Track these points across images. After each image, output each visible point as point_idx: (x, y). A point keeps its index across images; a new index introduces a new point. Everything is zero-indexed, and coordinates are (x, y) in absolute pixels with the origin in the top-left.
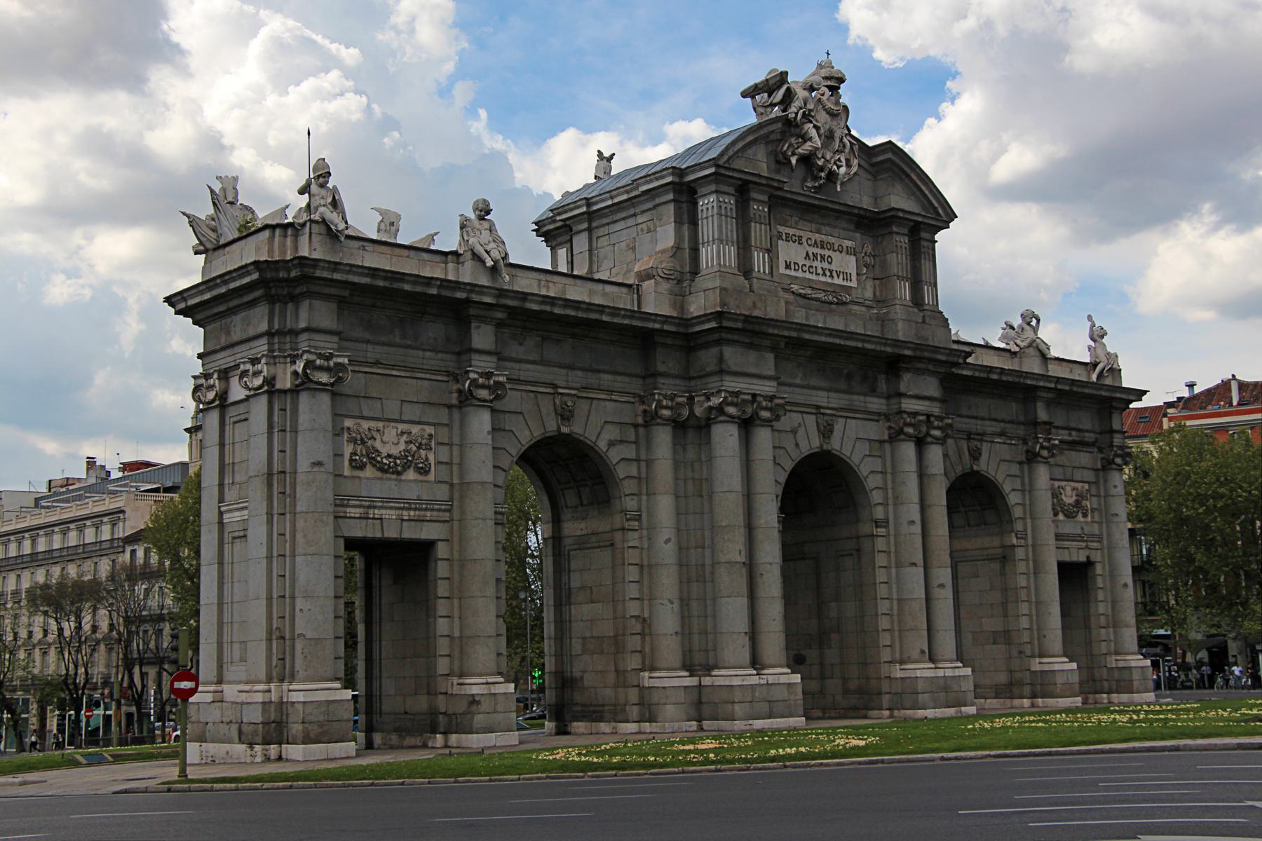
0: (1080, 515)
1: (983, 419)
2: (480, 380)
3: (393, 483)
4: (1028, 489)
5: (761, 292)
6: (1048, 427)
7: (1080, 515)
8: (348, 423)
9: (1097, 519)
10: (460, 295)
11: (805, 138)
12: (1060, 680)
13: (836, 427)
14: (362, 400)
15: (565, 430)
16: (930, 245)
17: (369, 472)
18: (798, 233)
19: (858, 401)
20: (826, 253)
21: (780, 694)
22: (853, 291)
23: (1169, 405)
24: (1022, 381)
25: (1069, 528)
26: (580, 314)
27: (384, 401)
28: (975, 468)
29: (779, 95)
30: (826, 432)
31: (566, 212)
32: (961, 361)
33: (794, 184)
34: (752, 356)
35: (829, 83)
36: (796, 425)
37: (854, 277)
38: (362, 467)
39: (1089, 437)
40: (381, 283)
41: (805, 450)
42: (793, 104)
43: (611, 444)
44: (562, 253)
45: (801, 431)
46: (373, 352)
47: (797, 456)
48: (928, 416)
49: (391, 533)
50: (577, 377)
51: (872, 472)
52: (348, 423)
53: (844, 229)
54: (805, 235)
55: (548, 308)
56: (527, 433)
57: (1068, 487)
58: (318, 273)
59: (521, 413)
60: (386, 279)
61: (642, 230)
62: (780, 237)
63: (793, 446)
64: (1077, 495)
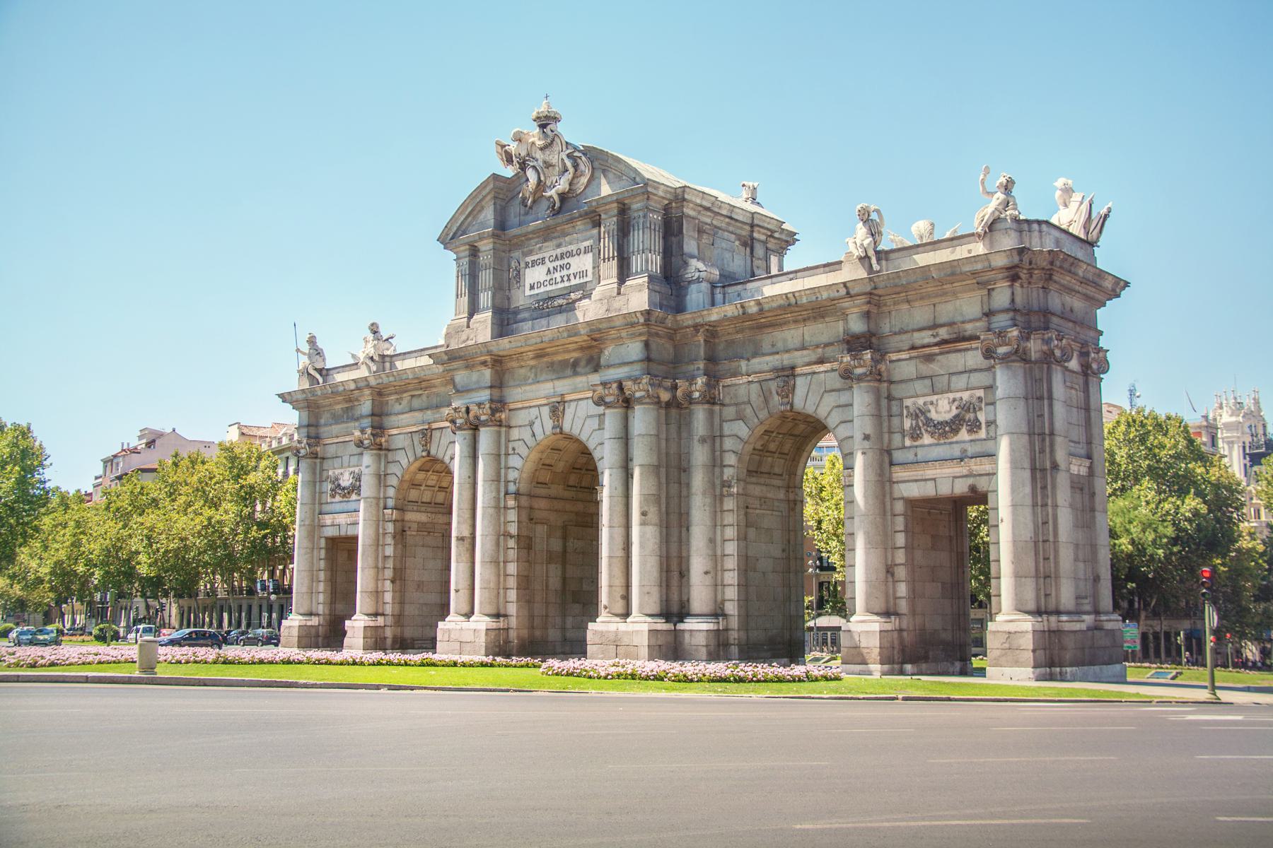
1: (787, 351)
8: (330, 473)
13: (567, 411)
17: (338, 498)
20: (565, 261)
21: (468, 637)
22: (588, 285)
34: (475, 376)
37: (590, 273)
45: (538, 422)
49: (343, 533)
50: (429, 415)
52: (330, 473)
54: (547, 255)
55: (380, 381)
59: (404, 449)
64: (957, 408)
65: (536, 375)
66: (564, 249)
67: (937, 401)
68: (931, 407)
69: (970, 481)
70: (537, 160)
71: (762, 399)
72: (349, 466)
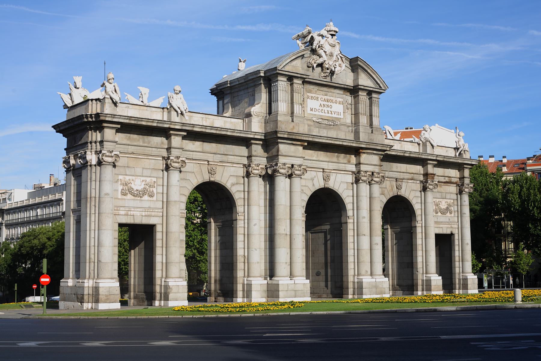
0: (448, 213)
1: (403, 173)
2: (175, 160)
3: (139, 201)
4: (425, 203)
5: (297, 122)
6: (433, 176)
7: (449, 212)
9: (456, 213)
10: (166, 126)
11: (320, 56)
12: (433, 283)
14: (126, 168)
15: (212, 179)
16: (377, 100)
17: (129, 196)
18: (316, 96)
19: (342, 167)
20: (329, 104)
22: (341, 120)
23: (529, 159)
24: (420, 156)
25: (441, 218)
26: (218, 132)
27: (136, 168)
28: (399, 194)
29: (309, 38)
30: (326, 179)
31: (221, 86)
32: (388, 149)
33: (316, 74)
35: (331, 33)
36: (314, 177)
37: (342, 114)
38: (125, 194)
39: (454, 180)
40: (133, 122)
41: (317, 187)
42: (314, 42)
43: (233, 185)
44: (221, 102)
45: (316, 179)
46: (131, 149)
47: (313, 190)
48: (373, 173)
49: (138, 221)
50: (218, 158)
51: (348, 196)
52: (121, 177)
53: (338, 93)
54: (320, 97)
55: (204, 130)
56: (196, 180)
57: (444, 201)
58: (107, 119)
60: (135, 120)
61: (250, 95)
62: (308, 97)
63: (311, 185)
65: (318, 156)
66: (328, 97)
67: (442, 201)
68: (440, 203)
69: (451, 230)
70: (325, 49)
71: (391, 188)
72: (143, 176)
